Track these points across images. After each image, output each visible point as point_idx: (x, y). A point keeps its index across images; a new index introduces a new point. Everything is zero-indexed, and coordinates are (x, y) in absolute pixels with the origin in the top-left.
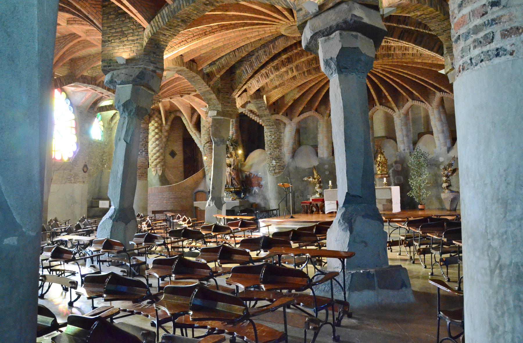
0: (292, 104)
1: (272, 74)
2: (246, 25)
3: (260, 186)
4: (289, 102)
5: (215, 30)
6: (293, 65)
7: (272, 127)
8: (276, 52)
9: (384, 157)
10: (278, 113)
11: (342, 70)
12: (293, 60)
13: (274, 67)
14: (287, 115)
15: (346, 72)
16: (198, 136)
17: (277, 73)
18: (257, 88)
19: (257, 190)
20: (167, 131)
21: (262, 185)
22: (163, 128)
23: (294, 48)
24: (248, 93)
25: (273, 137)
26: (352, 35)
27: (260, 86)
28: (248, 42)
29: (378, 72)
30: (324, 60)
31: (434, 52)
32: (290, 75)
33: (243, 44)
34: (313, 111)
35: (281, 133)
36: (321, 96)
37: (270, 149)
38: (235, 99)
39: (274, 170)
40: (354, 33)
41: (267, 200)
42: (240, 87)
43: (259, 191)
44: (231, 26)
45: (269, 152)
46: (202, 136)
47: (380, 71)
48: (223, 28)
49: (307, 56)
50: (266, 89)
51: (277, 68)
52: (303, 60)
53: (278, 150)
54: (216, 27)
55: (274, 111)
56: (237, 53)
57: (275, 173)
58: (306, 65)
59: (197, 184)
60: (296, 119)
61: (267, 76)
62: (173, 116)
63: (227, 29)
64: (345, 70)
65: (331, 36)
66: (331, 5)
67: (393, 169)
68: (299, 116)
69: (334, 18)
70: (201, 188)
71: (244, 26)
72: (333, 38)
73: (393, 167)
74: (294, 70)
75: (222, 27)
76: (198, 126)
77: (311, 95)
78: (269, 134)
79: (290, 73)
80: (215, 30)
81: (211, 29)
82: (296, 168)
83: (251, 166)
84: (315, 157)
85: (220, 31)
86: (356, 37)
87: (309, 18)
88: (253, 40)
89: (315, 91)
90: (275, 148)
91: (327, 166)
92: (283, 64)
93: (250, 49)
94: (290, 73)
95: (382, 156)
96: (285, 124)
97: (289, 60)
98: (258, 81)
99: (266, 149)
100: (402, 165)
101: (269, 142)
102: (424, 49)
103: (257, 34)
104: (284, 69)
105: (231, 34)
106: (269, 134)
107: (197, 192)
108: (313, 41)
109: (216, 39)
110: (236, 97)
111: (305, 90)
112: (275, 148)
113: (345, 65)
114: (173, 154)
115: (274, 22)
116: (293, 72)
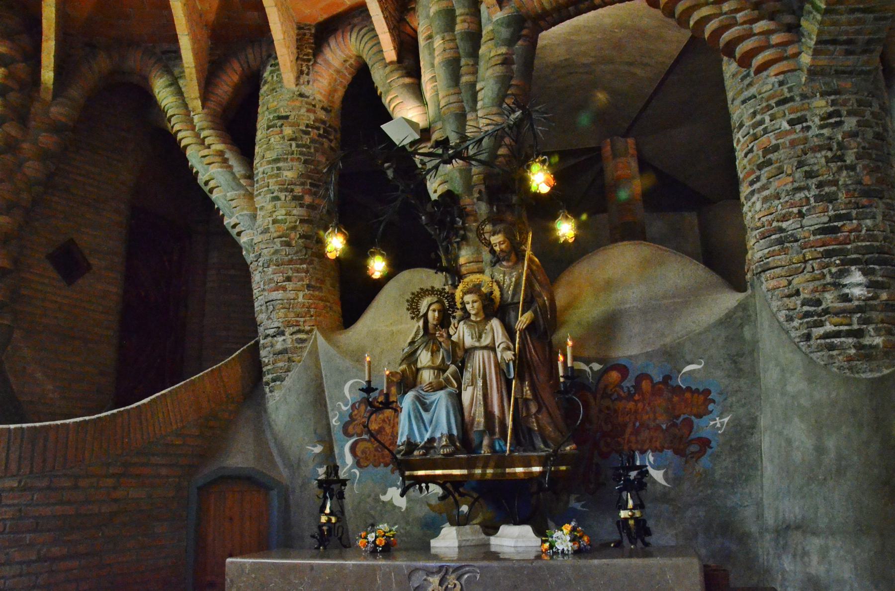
3: (686, 445)
16: (238, 169)
19: (657, 475)
20: (44, 155)
21: (705, 443)
22: (36, 108)
25: (851, 123)
37: (831, 199)
39: (859, 334)
41: (743, 538)
43: (675, 479)
46: (261, 167)
57: (866, 354)
59: (214, 431)
62: (102, 63)
70: (240, 457)
76: (238, 127)
78: (821, 105)
83: (608, 327)
90: (867, 193)
101: (818, 160)
106: (821, 105)
107: (214, 482)
112: (867, 193)
114: (70, 263)
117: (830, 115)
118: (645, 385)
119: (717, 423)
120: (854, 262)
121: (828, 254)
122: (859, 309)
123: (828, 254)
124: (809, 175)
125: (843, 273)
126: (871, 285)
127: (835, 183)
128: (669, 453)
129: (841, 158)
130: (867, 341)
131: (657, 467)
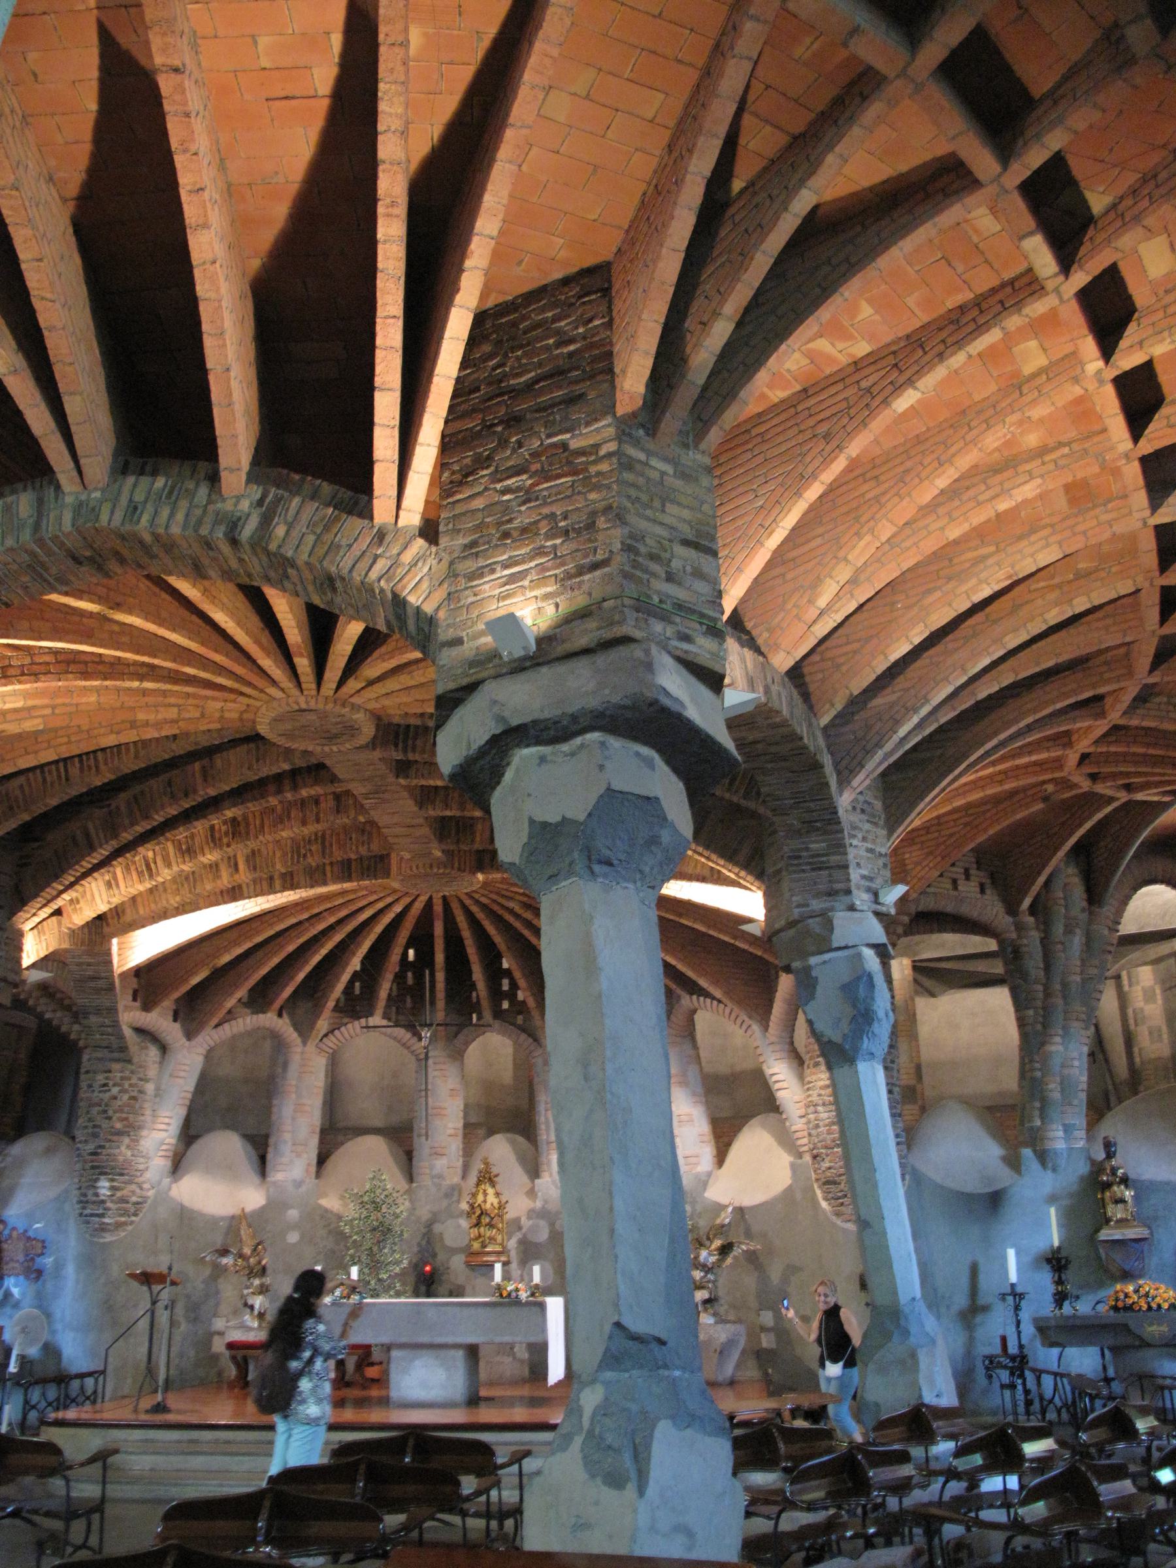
0: (206, 979)
1: (169, 866)
2: (151, 672)
4: (192, 973)
5: (43, 669)
6: (240, 851)
7: (116, 1055)
8: (212, 792)
9: (497, 1194)
10: (147, 1007)
11: (597, 868)
12: (252, 832)
13: (178, 846)
14: (175, 1020)
15: (605, 876)
17: (186, 868)
18: (103, 908)
19: (16, 1291)
21: (39, 1273)
23: (272, 788)
24: (65, 920)
26: (638, 754)
27: (116, 901)
28: (131, 736)
29: (511, 911)
30: (532, 822)
31: (736, 864)
32: (225, 880)
33: (110, 740)
34: (269, 1015)
35: (145, 1080)
36: (308, 968)
38: (21, 934)
40: (646, 751)
42: (49, 892)
44: (100, 667)
45: (90, 1147)
47: (517, 909)
48: (69, 664)
49: (304, 823)
50: (129, 917)
51: (188, 852)
52: (284, 834)
53: (126, 1140)
54: (47, 658)
55: (135, 1000)
56: (74, 771)
58: (285, 854)
60: (209, 1037)
61: (149, 870)
63: (86, 675)
64: (606, 869)
65: (565, 747)
66: (583, 642)
67: (519, 1235)
68: (216, 1026)
69: (591, 686)
71: (141, 678)
72: (573, 754)
73: (520, 1228)
74: (242, 866)
75: (68, 663)
77: (276, 961)
79: (225, 874)
80: (43, 669)
81: (28, 661)
82: (185, 1216)
84: (256, 1179)
85: (59, 675)
86: (651, 765)
87: (492, 672)
88: (151, 734)
89: (291, 948)
91: (293, 1214)
92: (214, 839)
93: (130, 765)
94: (225, 874)
95: (490, 1191)
96: (164, 1048)
97: (237, 829)
98: (109, 885)
99: (79, 1134)
100: (552, 1225)
102: (707, 853)
103: (173, 713)
104: (210, 857)
105: (89, 693)
108: (488, 758)
109: (30, 703)
110: (27, 927)
111: (259, 939)
113: (608, 852)
115: (249, 684)
116: (237, 870)
117: (105, 1085)
118: (15, 1234)
119: (48, 1261)
120: (106, 1174)
121: (93, 1168)
122: (103, 1202)
123: (93, 1168)
124: (90, 1120)
125: (97, 1180)
126: (112, 1188)
127: (99, 1126)
128: (21, 1278)
129: (105, 1112)
130: (107, 1220)
131: (16, 1286)
